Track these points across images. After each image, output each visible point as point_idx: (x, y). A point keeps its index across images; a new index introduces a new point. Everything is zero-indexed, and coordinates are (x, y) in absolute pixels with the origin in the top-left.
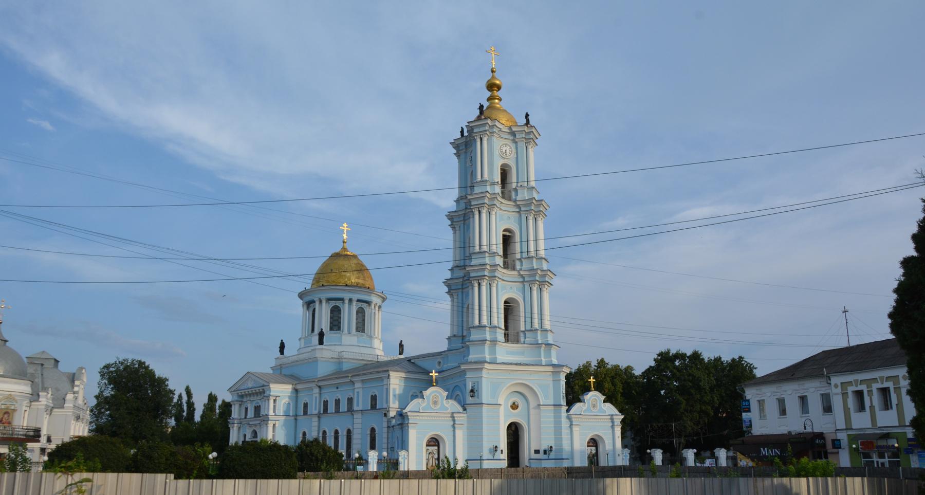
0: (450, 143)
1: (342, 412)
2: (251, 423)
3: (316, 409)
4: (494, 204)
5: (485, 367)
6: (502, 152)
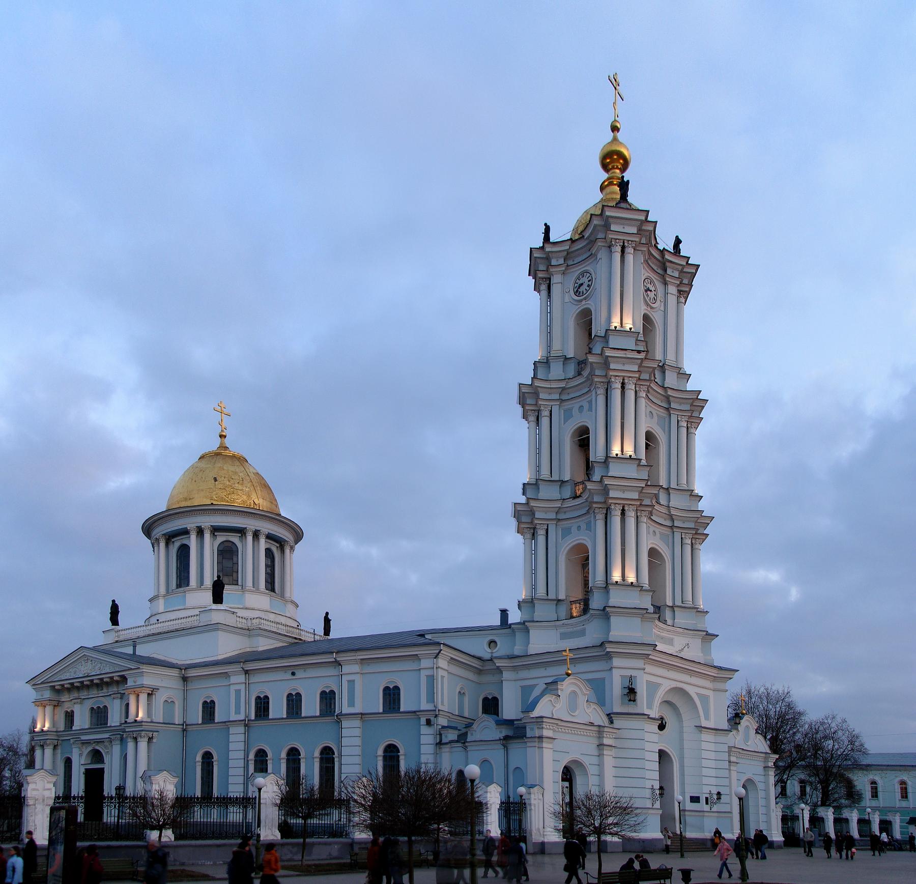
1: (272, 719)
2: (83, 738)
3: (238, 711)
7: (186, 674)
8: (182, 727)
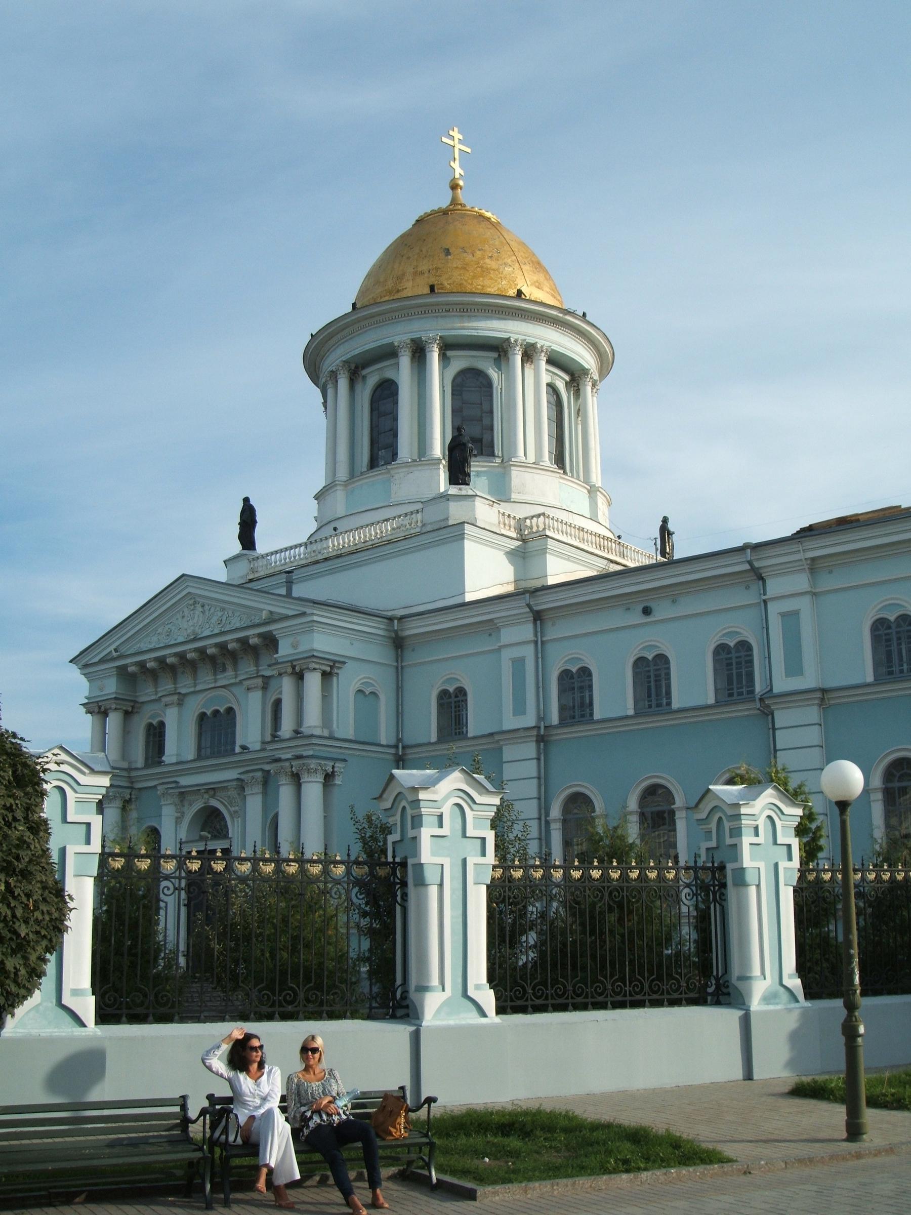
2: (185, 781)
3: (519, 709)
8: (393, 751)
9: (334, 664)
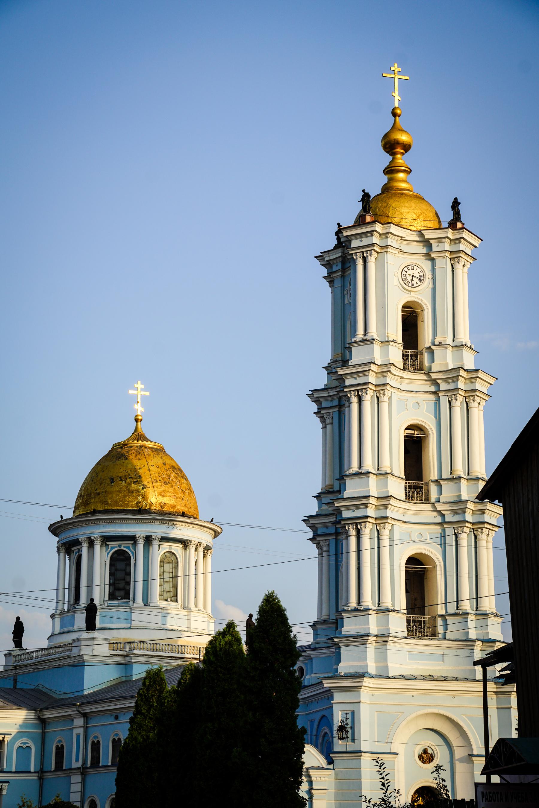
0: (316, 257)
4: (386, 384)
5: (364, 684)
6: (406, 279)
7: (43, 715)
9: (5, 736)
